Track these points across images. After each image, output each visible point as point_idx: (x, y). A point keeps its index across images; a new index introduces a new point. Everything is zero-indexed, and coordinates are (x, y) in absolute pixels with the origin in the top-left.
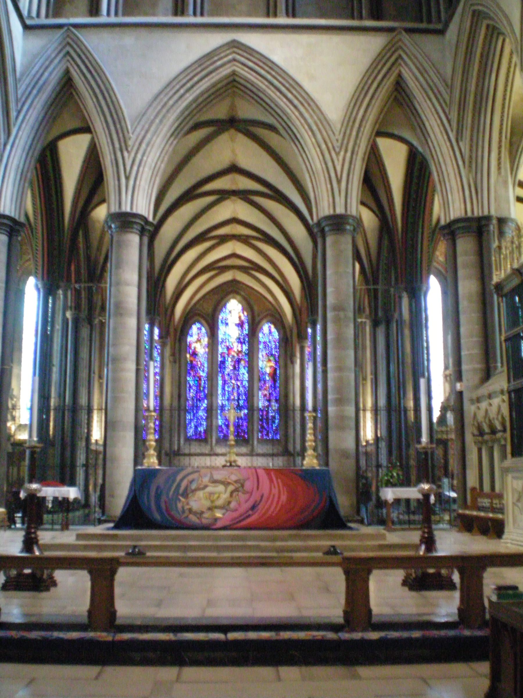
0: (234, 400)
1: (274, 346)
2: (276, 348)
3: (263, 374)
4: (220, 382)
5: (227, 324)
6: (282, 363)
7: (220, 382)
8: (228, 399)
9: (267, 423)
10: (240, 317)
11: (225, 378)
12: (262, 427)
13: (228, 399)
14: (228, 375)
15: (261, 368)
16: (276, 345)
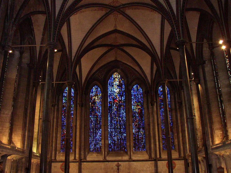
0: (118, 128)
1: (140, 97)
2: (141, 98)
3: (134, 113)
4: (109, 118)
5: (113, 86)
6: (145, 106)
7: (109, 118)
8: (114, 128)
9: (138, 142)
10: (120, 82)
11: (112, 115)
12: (135, 144)
13: (114, 128)
14: (114, 114)
15: (133, 110)
16: (141, 96)
